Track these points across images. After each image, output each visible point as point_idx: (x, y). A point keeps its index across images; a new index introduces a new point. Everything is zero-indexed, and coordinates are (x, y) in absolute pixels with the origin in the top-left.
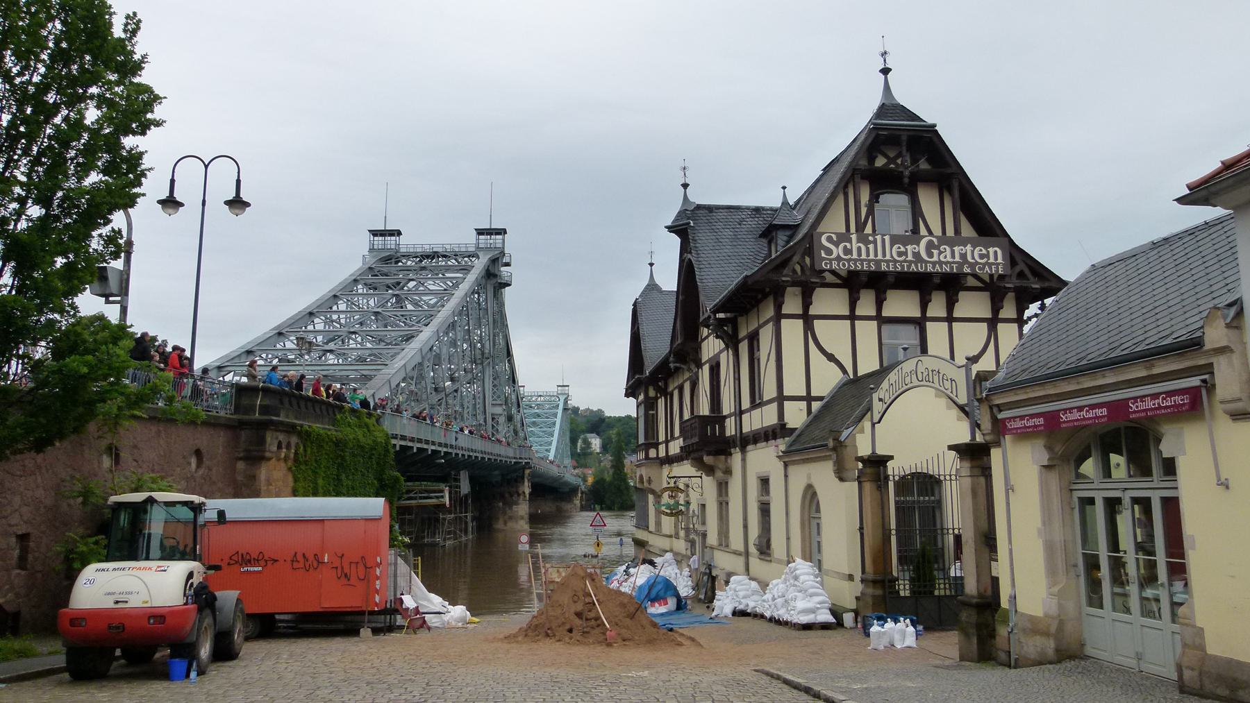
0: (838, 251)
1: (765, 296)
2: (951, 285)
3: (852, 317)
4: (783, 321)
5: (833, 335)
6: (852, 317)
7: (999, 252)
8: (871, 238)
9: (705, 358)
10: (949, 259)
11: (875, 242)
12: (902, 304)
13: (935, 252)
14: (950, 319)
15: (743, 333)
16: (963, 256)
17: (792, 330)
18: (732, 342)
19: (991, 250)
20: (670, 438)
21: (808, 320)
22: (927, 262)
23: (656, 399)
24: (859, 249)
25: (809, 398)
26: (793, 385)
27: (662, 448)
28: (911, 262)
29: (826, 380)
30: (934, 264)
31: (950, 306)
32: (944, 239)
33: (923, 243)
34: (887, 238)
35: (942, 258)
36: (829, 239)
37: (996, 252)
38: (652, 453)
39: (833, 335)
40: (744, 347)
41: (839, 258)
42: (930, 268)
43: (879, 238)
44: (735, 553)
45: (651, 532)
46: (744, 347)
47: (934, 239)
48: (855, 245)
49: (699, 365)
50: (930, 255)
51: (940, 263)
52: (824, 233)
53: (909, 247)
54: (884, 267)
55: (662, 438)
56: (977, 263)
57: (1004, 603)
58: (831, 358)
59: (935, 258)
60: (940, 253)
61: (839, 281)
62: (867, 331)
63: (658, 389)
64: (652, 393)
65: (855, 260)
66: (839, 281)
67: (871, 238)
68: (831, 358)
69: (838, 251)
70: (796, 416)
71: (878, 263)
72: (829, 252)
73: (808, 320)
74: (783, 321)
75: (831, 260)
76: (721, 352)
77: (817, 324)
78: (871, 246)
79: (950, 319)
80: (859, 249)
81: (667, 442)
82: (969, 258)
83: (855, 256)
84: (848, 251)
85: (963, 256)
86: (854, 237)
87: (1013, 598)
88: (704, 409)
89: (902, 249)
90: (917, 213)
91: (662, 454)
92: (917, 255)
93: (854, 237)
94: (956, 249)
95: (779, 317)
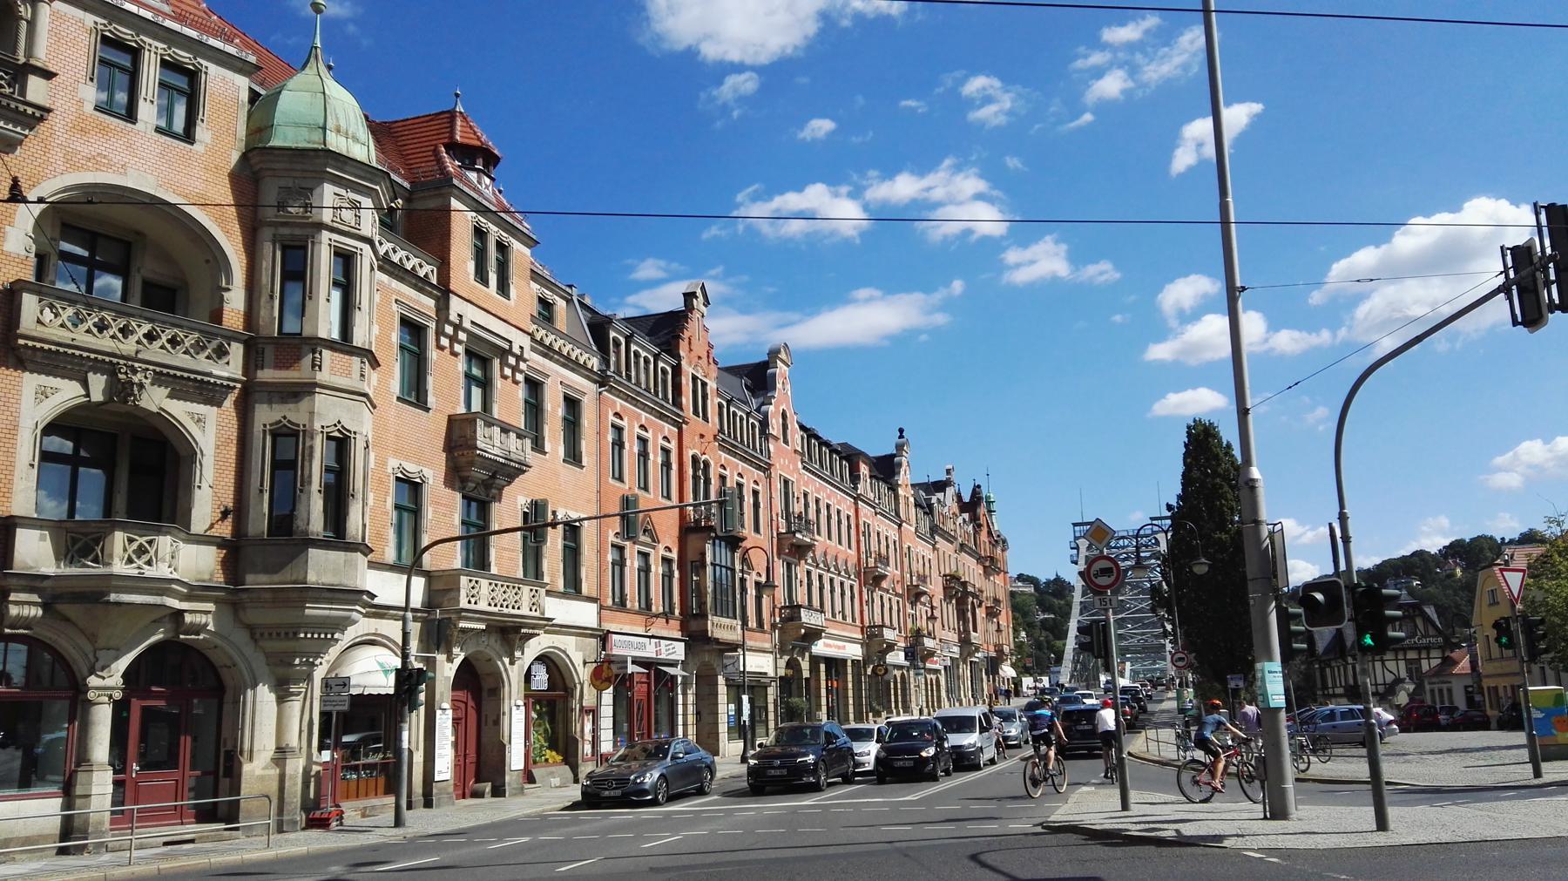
2: (1428, 648)
3: (1397, 660)
5: (1391, 665)
6: (1397, 660)
12: (1412, 655)
14: (1429, 658)
17: (1378, 665)
20: (1334, 686)
21: (1383, 662)
25: (1385, 684)
26: (1380, 680)
29: (1390, 678)
31: (1428, 654)
32: (1423, 636)
39: (1391, 665)
55: (1330, 685)
62: (1402, 664)
70: (1381, 689)
73: (1383, 662)
77: (1387, 663)
79: (1429, 658)
88: (1351, 682)
90: (1416, 626)
95: (1373, 661)
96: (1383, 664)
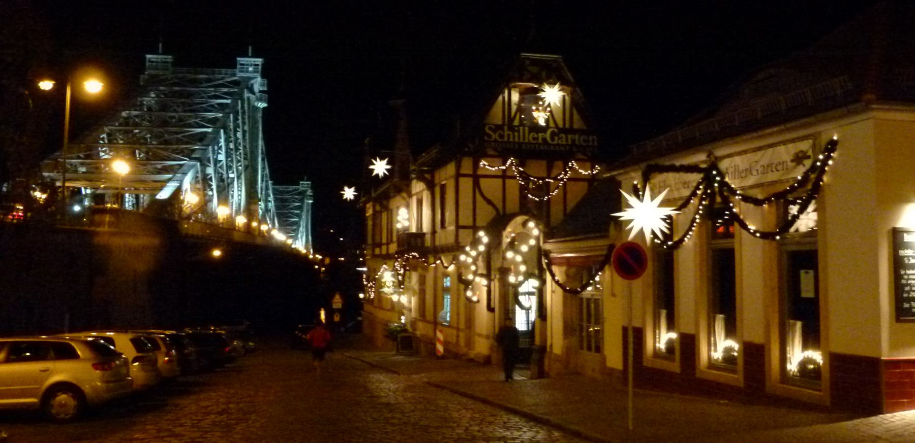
0: (495, 136)
1: (451, 161)
4: (462, 180)
5: (491, 187)
7: (595, 137)
8: (516, 128)
9: (414, 192)
10: (564, 143)
11: (519, 131)
12: (537, 169)
13: (556, 138)
15: (437, 181)
16: (573, 141)
18: (431, 186)
19: (591, 138)
22: (550, 145)
23: (381, 212)
24: (509, 135)
27: (384, 248)
28: (539, 144)
30: (555, 145)
33: (549, 131)
34: (527, 129)
35: (560, 142)
36: (490, 128)
37: (593, 139)
38: (377, 251)
40: (437, 190)
41: (495, 141)
42: (552, 148)
43: (521, 128)
44: (428, 322)
45: (376, 307)
46: (437, 190)
47: (556, 130)
48: (506, 133)
49: (410, 195)
50: (553, 140)
51: (558, 145)
52: (488, 124)
53: (540, 135)
54: (524, 147)
55: (384, 241)
56: (581, 145)
57: (548, 349)
58: (489, 202)
59: (556, 142)
60: (559, 138)
61: (497, 154)
63: (382, 206)
64: (378, 208)
65: (506, 142)
66: (497, 154)
67: (516, 128)
68: (489, 202)
69: (495, 136)
71: (520, 144)
72: (489, 136)
73: (476, 178)
74: (462, 180)
75: (490, 142)
76: (423, 190)
77: (483, 182)
78: (516, 134)
80: (509, 135)
81: (388, 244)
82: (577, 142)
83: (506, 139)
84: (501, 136)
85: (573, 141)
86: (506, 128)
87: (551, 346)
89: (536, 136)
91: (384, 252)
92: (544, 139)
93: (506, 128)
94: (569, 136)
96: (476, 184)
